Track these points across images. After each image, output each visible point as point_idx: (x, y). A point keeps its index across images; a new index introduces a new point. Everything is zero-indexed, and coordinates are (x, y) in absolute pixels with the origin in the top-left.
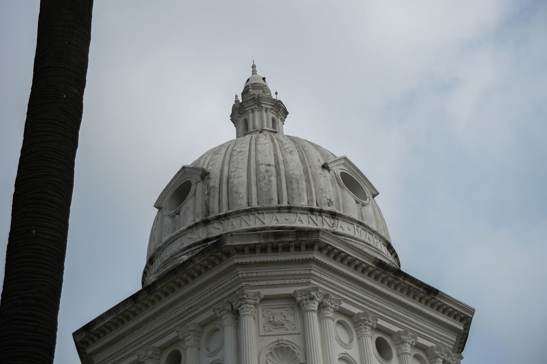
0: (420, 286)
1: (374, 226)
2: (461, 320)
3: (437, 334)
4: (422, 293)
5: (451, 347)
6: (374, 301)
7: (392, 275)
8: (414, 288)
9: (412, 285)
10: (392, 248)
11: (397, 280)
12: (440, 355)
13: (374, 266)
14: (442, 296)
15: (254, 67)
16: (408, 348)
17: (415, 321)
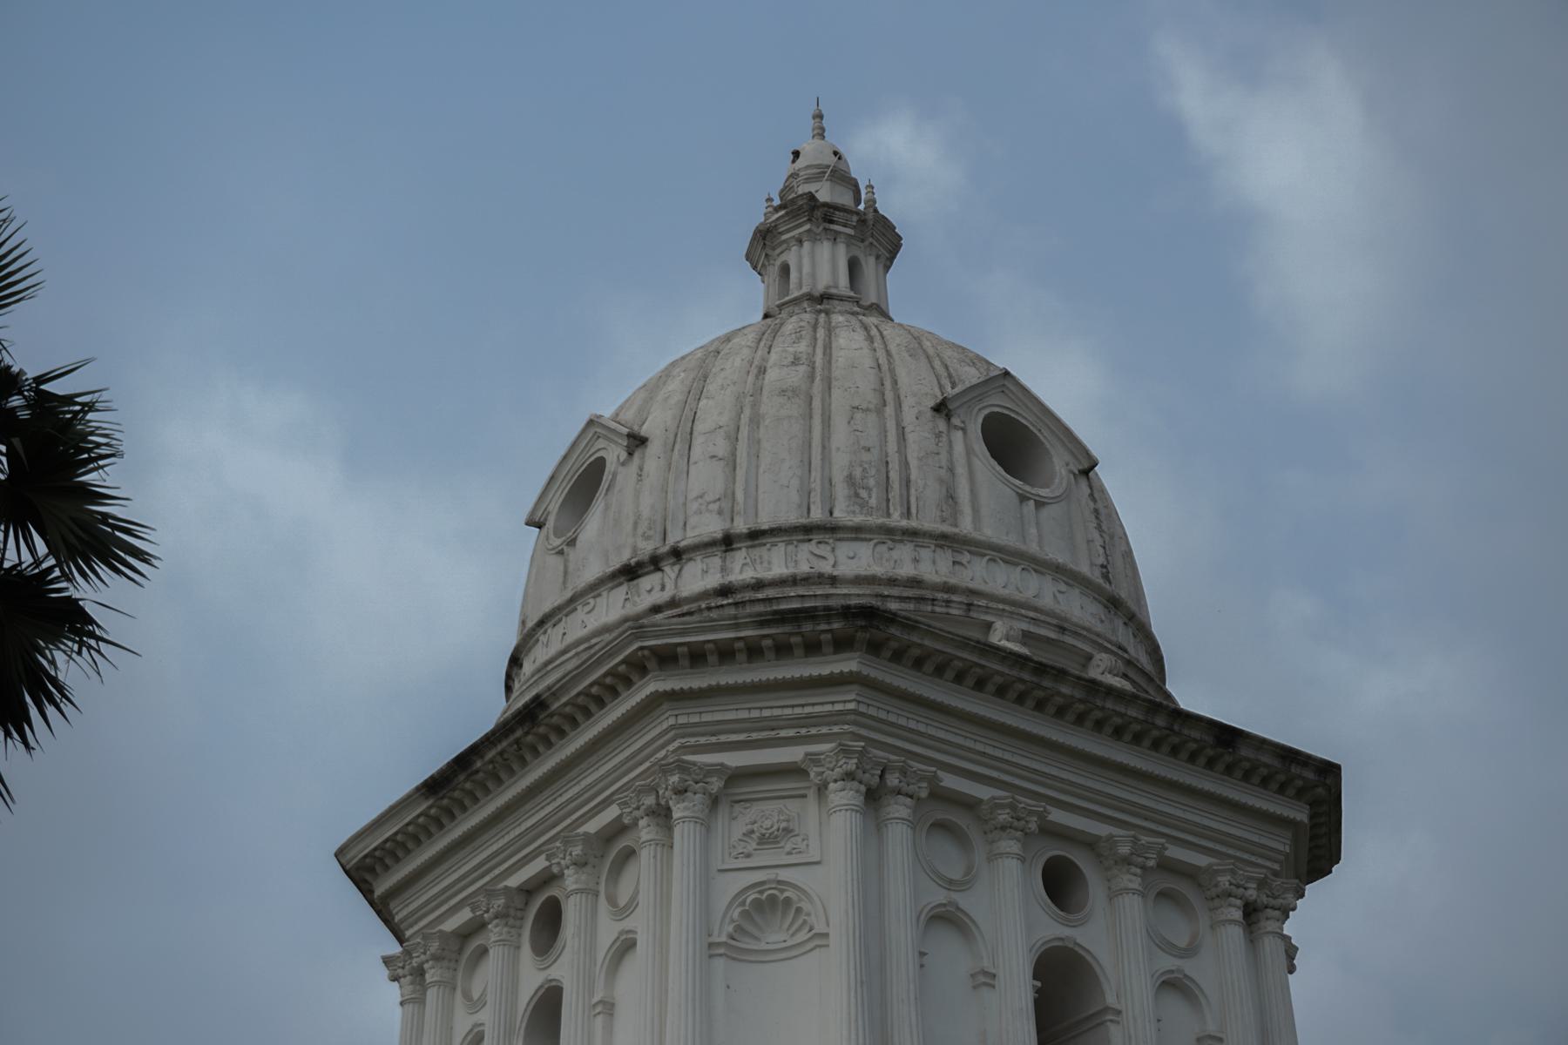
0: (512, 731)
1: (594, 570)
2: (638, 667)
3: (628, 759)
4: (527, 733)
5: (676, 744)
6: (495, 847)
7: (462, 777)
8: (510, 745)
9: (499, 748)
10: (640, 565)
11: (477, 772)
12: (636, 813)
13: (430, 802)
14: (554, 694)
15: (819, 116)
16: (571, 880)
17: (576, 789)
